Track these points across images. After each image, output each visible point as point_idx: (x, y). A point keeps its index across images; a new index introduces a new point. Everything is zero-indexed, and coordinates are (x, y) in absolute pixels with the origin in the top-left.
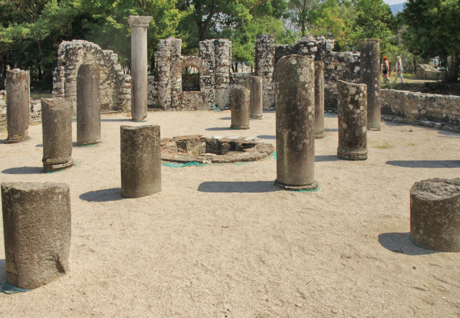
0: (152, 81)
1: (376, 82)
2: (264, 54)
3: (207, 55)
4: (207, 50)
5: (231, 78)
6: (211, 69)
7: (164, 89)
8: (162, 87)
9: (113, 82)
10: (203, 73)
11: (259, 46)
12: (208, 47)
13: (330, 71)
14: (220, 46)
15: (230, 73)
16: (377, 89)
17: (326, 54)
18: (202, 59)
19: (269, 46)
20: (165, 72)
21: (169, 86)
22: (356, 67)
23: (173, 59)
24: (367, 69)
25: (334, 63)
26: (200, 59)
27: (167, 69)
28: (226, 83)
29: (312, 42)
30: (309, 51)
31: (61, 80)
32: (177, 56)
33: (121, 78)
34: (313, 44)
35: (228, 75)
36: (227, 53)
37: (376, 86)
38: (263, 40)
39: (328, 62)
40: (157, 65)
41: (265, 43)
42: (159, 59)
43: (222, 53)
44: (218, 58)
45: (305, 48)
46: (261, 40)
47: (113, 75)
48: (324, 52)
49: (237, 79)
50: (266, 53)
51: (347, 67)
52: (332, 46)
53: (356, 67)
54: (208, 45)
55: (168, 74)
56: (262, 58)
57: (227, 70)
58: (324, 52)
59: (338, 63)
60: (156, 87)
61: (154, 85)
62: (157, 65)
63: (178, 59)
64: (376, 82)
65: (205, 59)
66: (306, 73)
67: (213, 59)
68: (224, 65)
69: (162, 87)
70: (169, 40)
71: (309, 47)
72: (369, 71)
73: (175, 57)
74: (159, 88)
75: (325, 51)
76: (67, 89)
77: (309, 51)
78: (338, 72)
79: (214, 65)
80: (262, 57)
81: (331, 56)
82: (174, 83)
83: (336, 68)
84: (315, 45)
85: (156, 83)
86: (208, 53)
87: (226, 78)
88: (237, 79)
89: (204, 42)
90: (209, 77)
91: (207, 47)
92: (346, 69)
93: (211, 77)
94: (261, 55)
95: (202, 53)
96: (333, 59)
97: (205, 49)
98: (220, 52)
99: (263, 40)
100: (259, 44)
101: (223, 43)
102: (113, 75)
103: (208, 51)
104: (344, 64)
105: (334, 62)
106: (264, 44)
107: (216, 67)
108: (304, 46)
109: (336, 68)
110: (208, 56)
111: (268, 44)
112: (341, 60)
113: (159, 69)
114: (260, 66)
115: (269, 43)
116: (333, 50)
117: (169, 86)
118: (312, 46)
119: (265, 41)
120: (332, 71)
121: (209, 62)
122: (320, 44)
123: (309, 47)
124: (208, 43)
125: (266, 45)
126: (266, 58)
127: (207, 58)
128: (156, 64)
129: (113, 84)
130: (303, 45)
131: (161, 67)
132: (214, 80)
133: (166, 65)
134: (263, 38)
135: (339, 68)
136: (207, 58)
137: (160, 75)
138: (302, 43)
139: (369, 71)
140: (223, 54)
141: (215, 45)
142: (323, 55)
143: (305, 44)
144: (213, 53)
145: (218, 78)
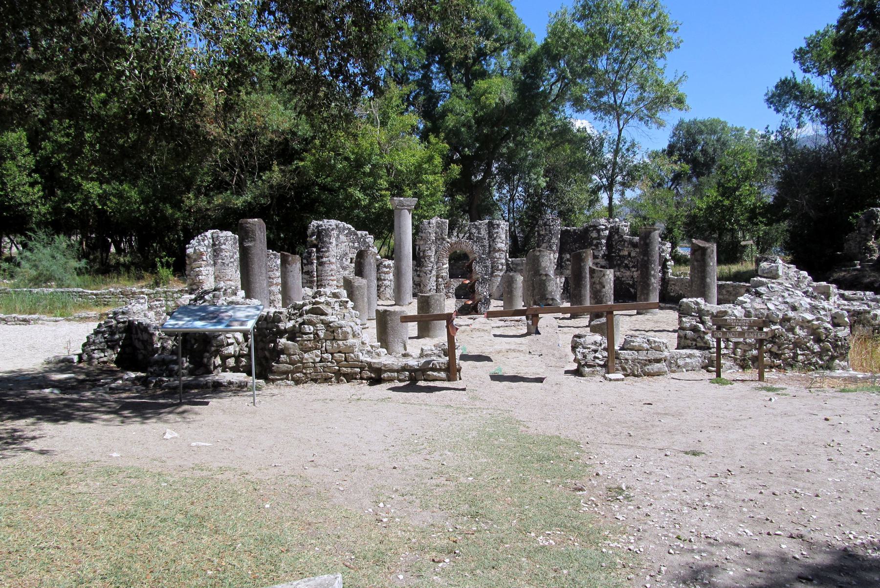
1: (653, 269)
2: (546, 238)
3: (478, 238)
4: (479, 233)
5: (507, 265)
7: (429, 276)
14: (494, 228)
15: (506, 259)
16: (654, 276)
21: (434, 272)
27: (432, 253)
28: (501, 270)
30: (599, 235)
31: (312, 263)
32: (444, 239)
35: (504, 261)
36: (503, 236)
37: (653, 272)
42: (422, 242)
48: (616, 237)
52: (627, 230)
55: (432, 259)
57: (503, 256)
58: (616, 237)
64: (653, 269)
68: (499, 250)
70: (433, 221)
71: (598, 231)
72: (646, 258)
74: (421, 274)
76: (319, 273)
81: (624, 241)
82: (439, 269)
84: (606, 229)
87: (502, 264)
91: (478, 229)
94: (543, 240)
96: (626, 244)
101: (498, 225)
107: (490, 252)
110: (480, 239)
113: (421, 254)
117: (434, 272)
118: (603, 230)
121: (482, 246)
122: (612, 227)
131: (424, 251)
133: (430, 249)
135: (633, 254)
138: (591, 226)
139: (646, 258)
144: (486, 237)
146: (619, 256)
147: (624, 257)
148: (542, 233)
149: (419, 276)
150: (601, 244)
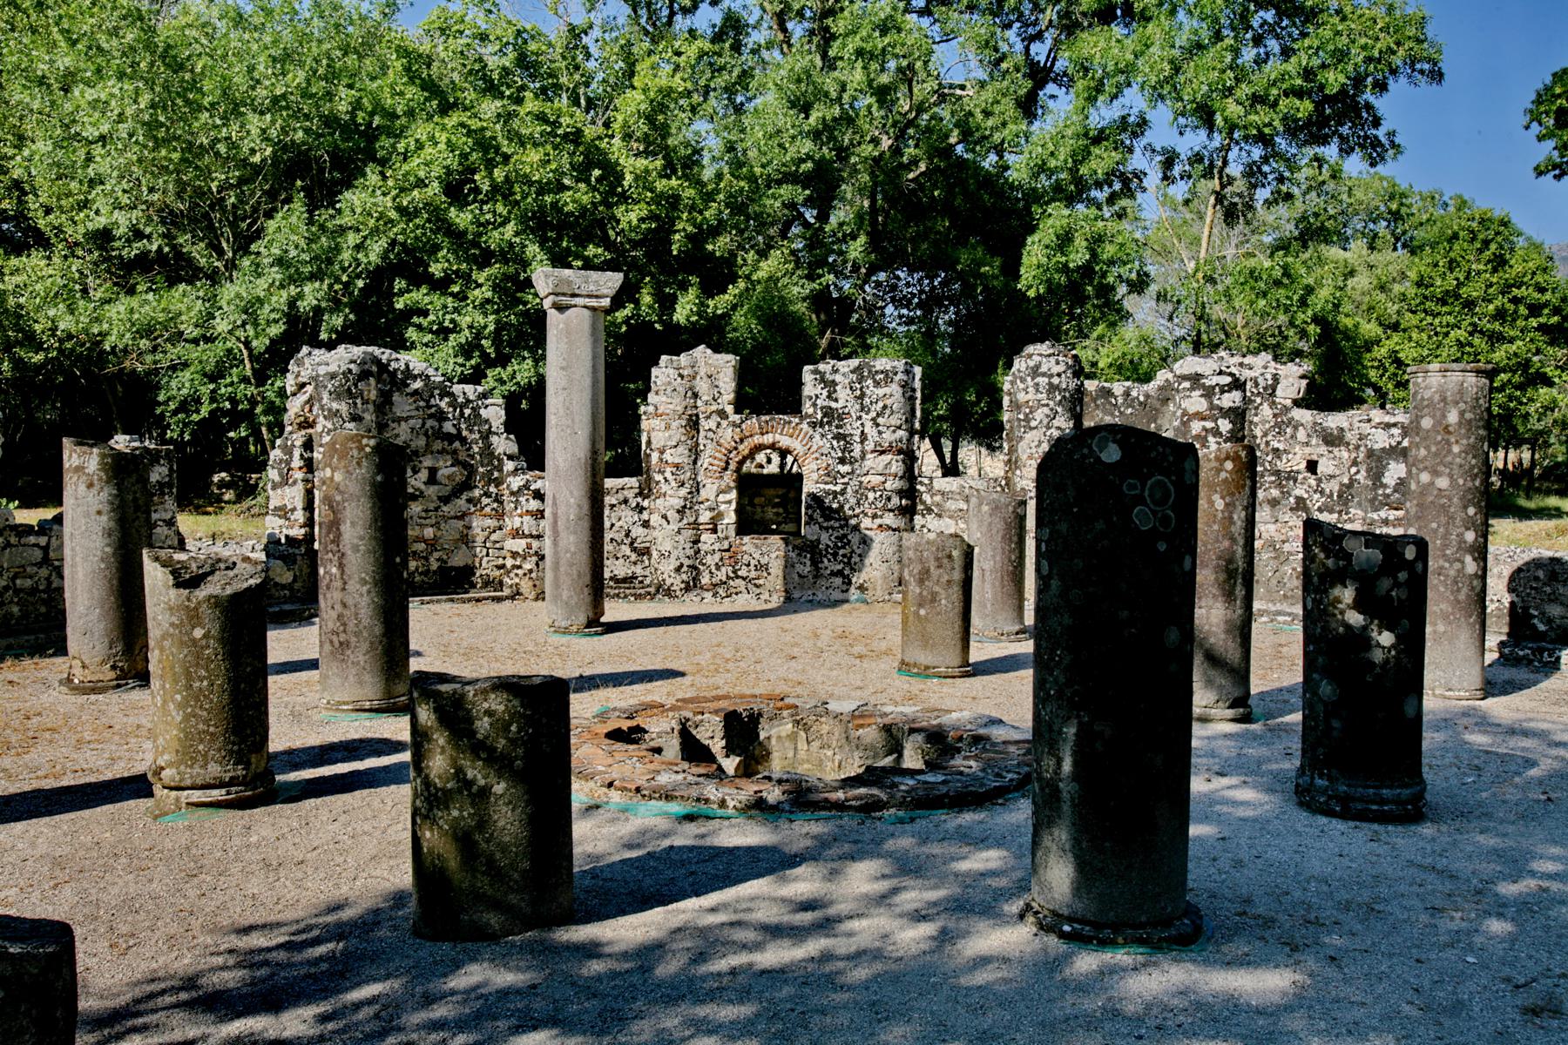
0: (630, 494)
2: (1040, 414)
3: (828, 412)
6: (842, 461)
8: (665, 517)
9: (487, 494)
10: (815, 476)
11: (1022, 386)
12: (834, 383)
13: (1288, 479)
14: (877, 384)
17: (1275, 416)
18: (813, 425)
19: (1057, 387)
20: (677, 466)
22: (1393, 465)
23: (712, 424)
24: (1435, 473)
25: (1307, 450)
26: (805, 426)
29: (1221, 373)
32: (722, 414)
33: (516, 482)
34: (1228, 379)
38: (1038, 366)
39: (1281, 446)
40: (649, 443)
41: (1044, 375)
42: (655, 422)
43: (885, 407)
44: (868, 425)
45: (1197, 393)
46: (1031, 364)
47: (490, 473)
48: (1266, 411)
49: (938, 498)
50: (1046, 410)
51: (1355, 463)
53: (1393, 465)
54: (838, 378)
56: (1032, 429)
59: (1323, 449)
60: (645, 516)
61: (640, 509)
62: (649, 443)
63: (724, 423)
65: (822, 426)
66: (1158, 495)
67: (852, 428)
69: (665, 517)
73: (716, 418)
74: (655, 520)
75: (1273, 404)
77: (1212, 407)
78: (1319, 481)
79: (857, 448)
80: (1033, 424)
83: (1312, 466)
84: (1237, 384)
85: (646, 503)
86: (834, 405)
88: (938, 498)
89: (821, 367)
90: (838, 488)
91: (831, 386)
92: (1354, 470)
93: (843, 492)
94: (1027, 419)
95: (814, 405)
97: (825, 393)
98: (880, 404)
99: (1038, 366)
100: (1023, 380)
102: (490, 473)
103: (836, 400)
104: (1345, 455)
105: (1307, 444)
106: (1043, 381)
107: (864, 453)
108: (1192, 389)
109: (1312, 466)
111: (1056, 380)
112: (1333, 440)
113: (655, 457)
114: (1024, 457)
115: (1059, 375)
116: (1297, 403)
119: (1044, 369)
120: (1295, 480)
121: (838, 437)
123: (1209, 393)
124: (836, 371)
125: (1050, 384)
126: (1048, 428)
127: (829, 423)
128: (644, 439)
129: (485, 501)
130: (1187, 384)
132: (853, 501)
134: (1036, 358)
135: (1324, 467)
136: (829, 423)
137: (658, 477)
138: (1184, 378)
140: (888, 412)
141: (861, 380)
142: (1264, 422)
143: (1196, 379)
144: (854, 409)
145: (871, 495)
146: (1277, 473)
147: (1292, 476)
148: (1022, 397)
149: (646, 524)
150: (1216, 432)
